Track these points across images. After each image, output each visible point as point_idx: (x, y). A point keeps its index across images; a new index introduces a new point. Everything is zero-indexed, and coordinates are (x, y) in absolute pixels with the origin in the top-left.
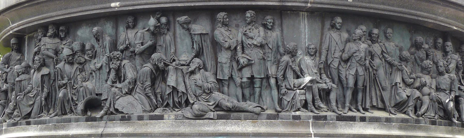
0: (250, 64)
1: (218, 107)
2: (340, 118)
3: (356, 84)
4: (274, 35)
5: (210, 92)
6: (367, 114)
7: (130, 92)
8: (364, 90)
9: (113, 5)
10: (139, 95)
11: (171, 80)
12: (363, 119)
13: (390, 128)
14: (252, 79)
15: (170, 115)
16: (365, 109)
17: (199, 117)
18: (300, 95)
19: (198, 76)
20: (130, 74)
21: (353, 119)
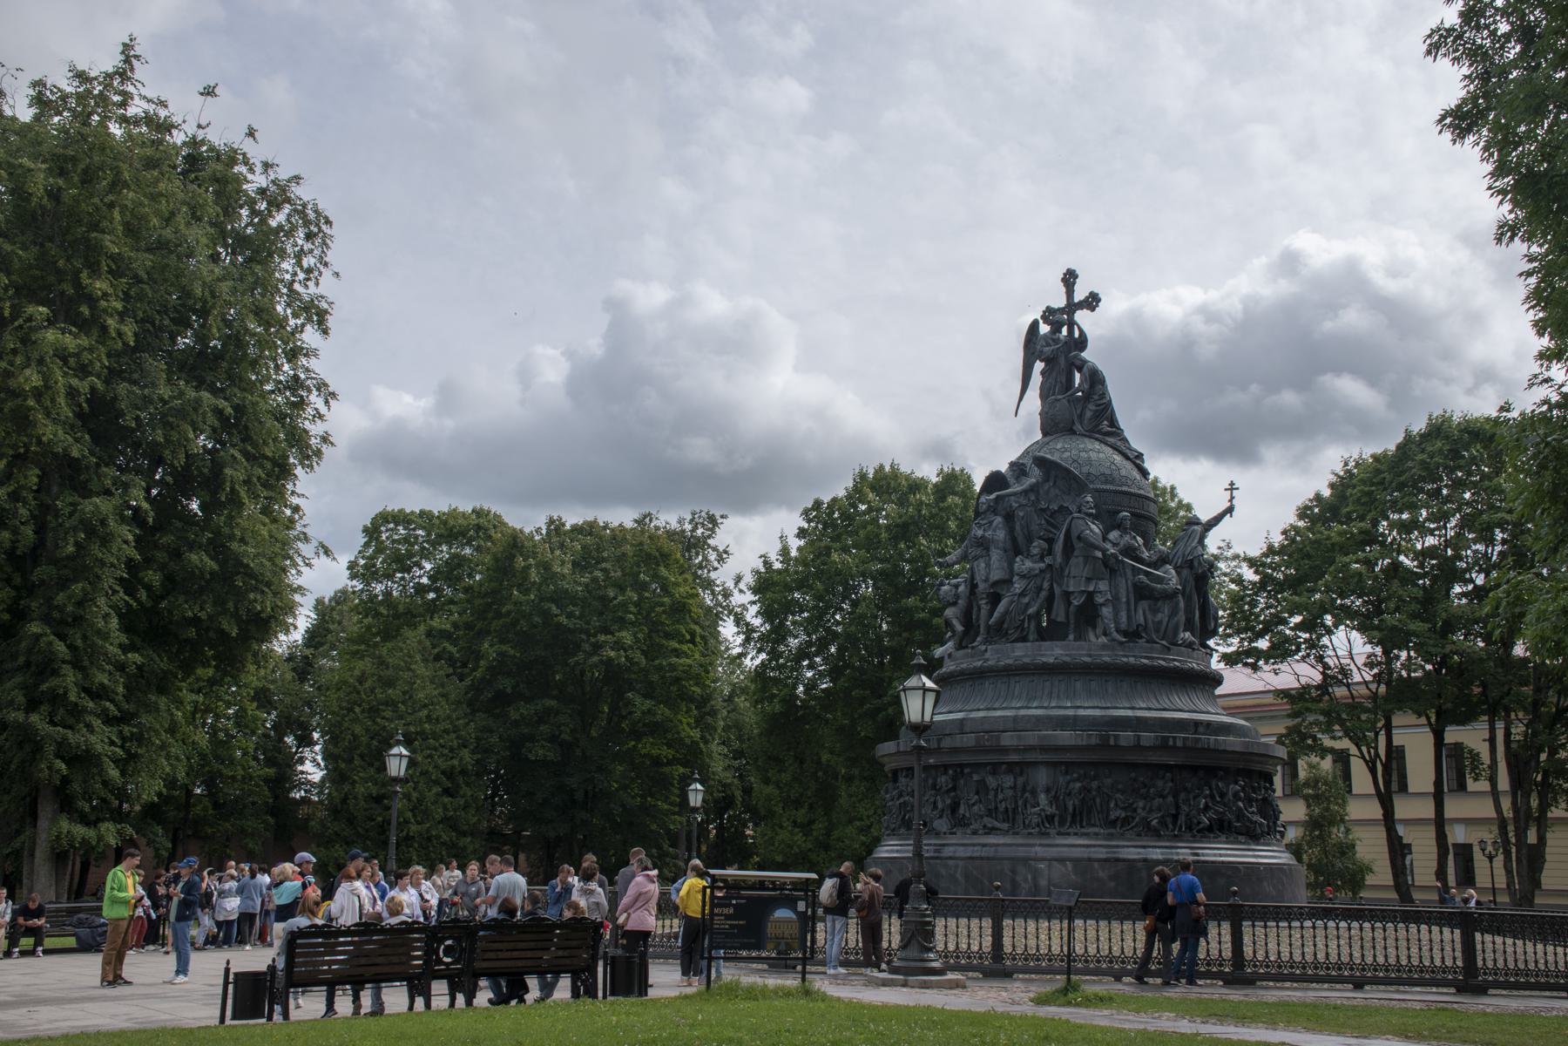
0: (1004, 800)
1: (985, 826)
2: (1059, 834)
3: (1074, 810)
4: (1020, 781)
5: (982, 817)
6: (1083, 830)
7: (941, 817)
8: (1081, 814)
9: (931, 761)
10: (945, 819)
11: (961, 811)
12: (1076, 834)
13: (1097, 839)
14: (1006, 808)
15: (959, 832)
16: (1082, 827)
17: (975, 833)
18: (1035, 820)
19: (976, 807)
20: (940, 805)
21: (1068, 834)
